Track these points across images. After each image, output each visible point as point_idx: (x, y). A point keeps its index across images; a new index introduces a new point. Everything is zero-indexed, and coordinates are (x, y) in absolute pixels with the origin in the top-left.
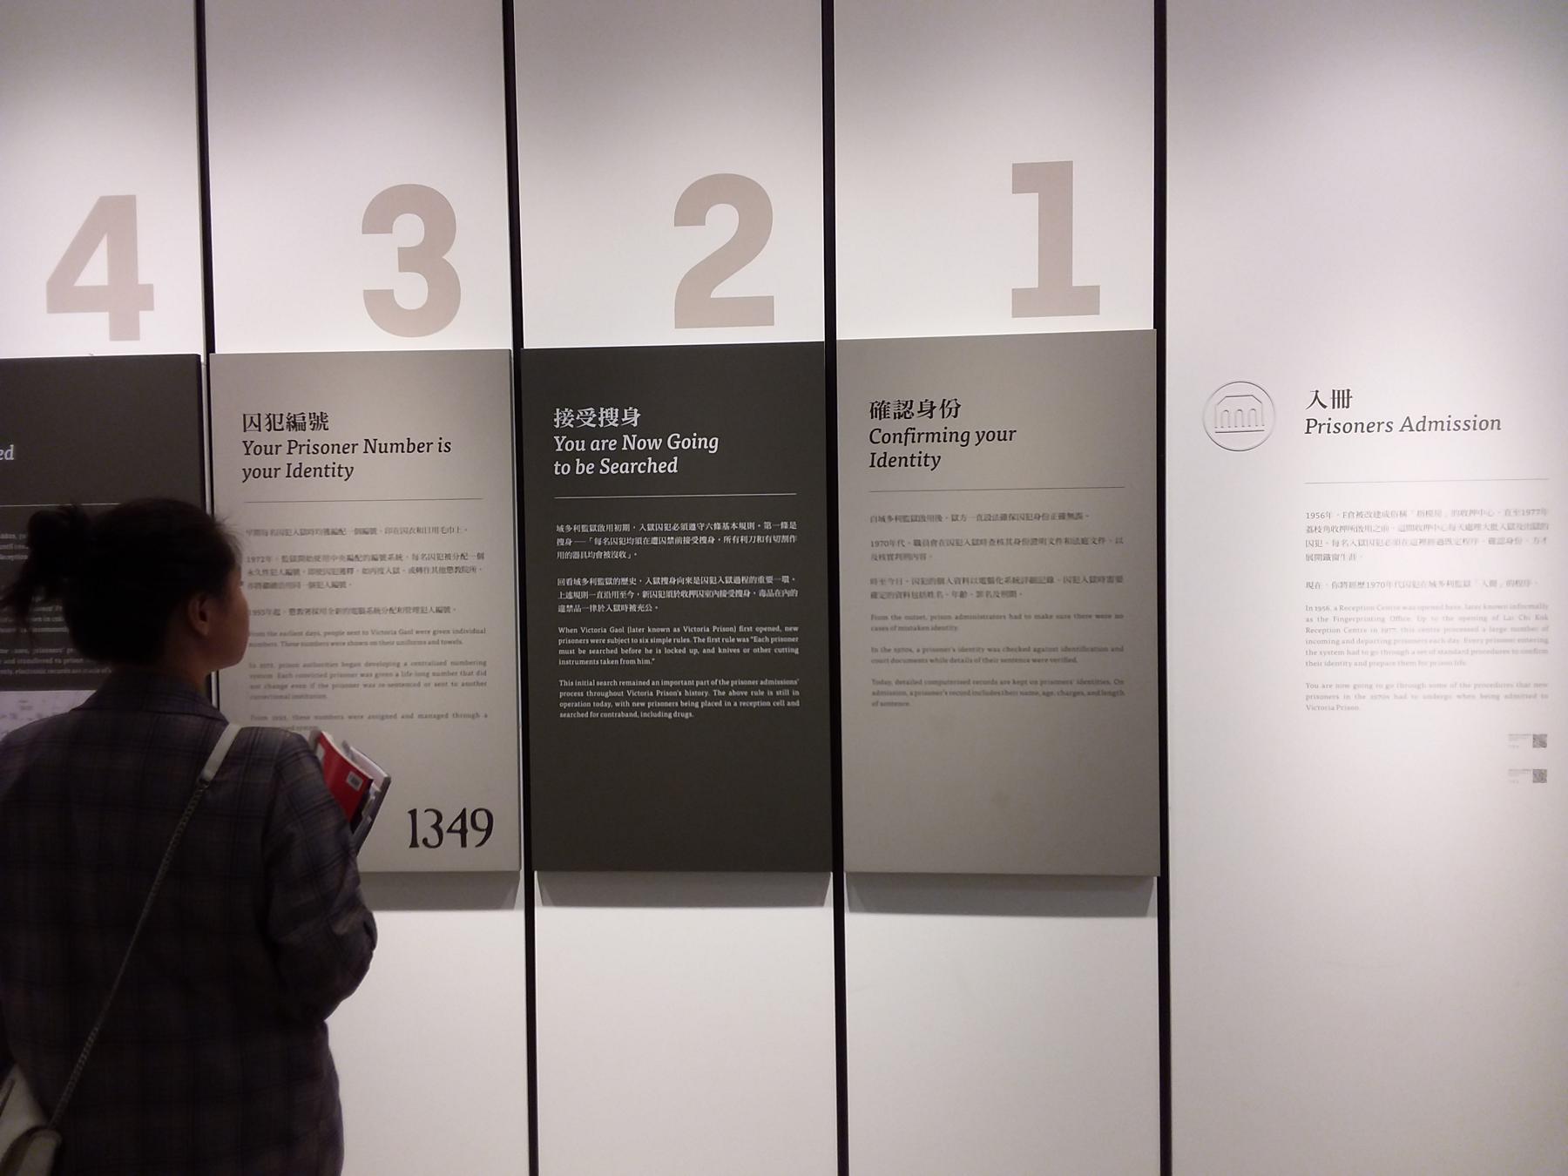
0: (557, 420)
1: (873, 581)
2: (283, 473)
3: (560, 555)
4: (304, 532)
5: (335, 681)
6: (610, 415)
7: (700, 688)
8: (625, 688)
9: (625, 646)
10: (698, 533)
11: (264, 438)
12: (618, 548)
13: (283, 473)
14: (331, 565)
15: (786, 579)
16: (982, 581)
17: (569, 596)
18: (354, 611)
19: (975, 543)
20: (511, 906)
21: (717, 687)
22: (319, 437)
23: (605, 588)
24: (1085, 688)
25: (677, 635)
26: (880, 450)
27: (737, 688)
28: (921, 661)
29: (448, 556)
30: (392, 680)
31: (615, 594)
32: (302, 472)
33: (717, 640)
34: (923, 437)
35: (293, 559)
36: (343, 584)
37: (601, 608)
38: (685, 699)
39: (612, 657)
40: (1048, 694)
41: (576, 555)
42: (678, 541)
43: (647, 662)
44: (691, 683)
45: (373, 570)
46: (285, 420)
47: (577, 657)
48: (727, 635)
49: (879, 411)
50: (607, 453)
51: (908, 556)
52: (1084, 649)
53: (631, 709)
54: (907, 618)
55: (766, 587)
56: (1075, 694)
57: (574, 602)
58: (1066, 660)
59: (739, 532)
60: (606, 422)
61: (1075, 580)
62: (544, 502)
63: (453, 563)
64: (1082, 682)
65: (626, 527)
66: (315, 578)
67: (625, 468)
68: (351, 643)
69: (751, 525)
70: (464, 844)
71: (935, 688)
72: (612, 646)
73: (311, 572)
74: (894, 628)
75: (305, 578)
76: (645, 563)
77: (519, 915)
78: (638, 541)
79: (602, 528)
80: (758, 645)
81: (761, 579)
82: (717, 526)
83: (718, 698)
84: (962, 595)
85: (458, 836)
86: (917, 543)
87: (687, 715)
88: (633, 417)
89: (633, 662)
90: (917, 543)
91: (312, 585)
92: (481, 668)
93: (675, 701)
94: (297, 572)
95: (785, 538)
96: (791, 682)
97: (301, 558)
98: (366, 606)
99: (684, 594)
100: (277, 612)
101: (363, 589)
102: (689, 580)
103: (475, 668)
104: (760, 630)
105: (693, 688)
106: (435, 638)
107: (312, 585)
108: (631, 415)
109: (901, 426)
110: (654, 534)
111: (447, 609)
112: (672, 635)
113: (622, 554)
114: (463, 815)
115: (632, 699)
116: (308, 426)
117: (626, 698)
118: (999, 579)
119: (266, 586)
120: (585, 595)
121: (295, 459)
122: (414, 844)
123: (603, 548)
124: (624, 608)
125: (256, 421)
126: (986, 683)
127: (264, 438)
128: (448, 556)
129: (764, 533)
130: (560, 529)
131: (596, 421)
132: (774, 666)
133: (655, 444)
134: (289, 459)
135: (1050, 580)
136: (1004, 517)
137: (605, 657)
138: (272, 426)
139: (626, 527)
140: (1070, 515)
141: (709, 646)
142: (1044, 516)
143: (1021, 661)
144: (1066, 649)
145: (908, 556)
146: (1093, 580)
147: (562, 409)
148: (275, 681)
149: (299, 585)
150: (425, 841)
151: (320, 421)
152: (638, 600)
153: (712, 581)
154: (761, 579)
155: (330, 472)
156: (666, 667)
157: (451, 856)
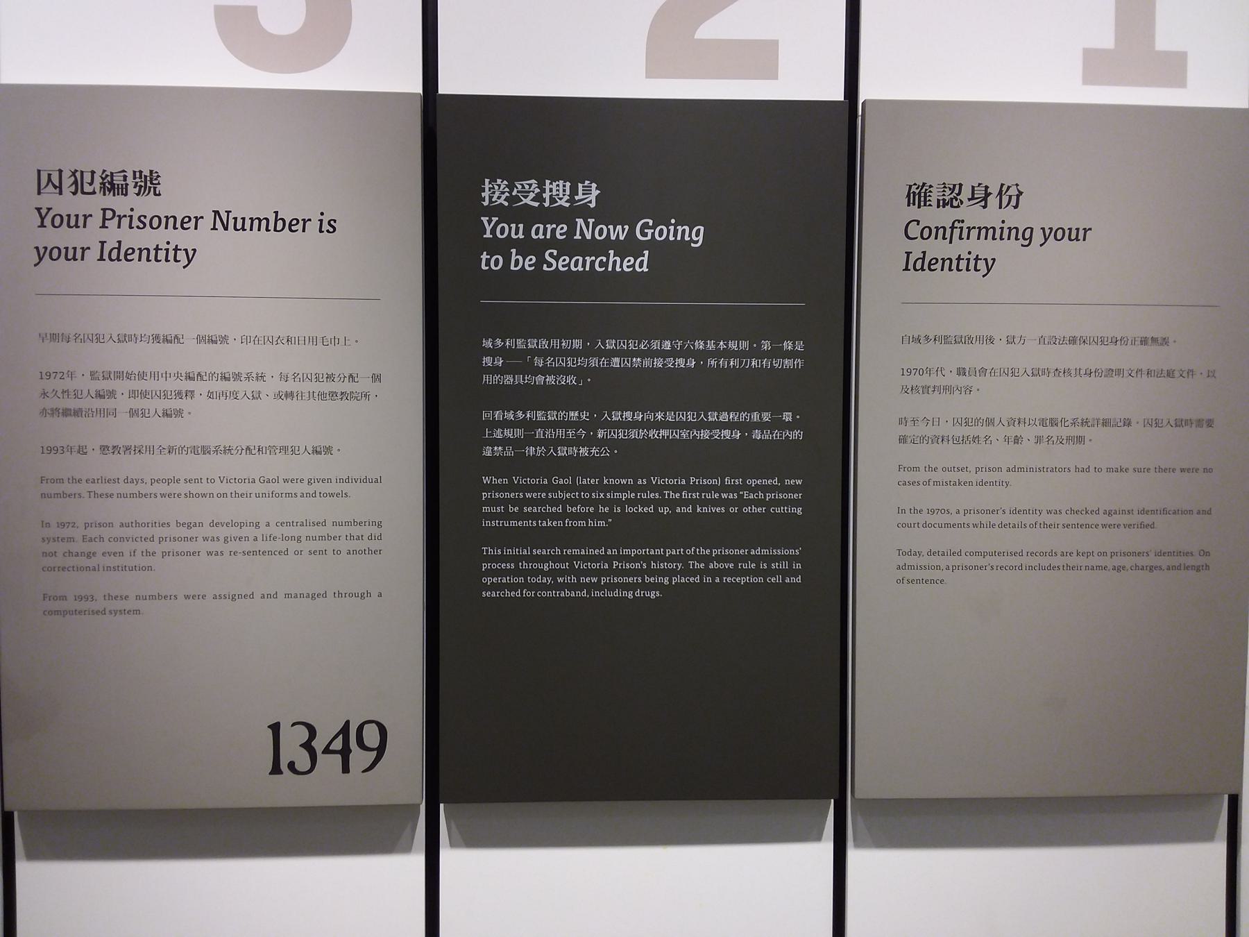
0: (486, 194)
1: (902, 421)
3: (487, 379)
4: (123, 339)
5: (166, 546)
6: (558, 191)
7: (672, 559)
8: (571, 558)
9: (573, 503)
10: (674, 353)
11: (68, 204)
12: (566, 371)
13: (94, 253)
14: (161, 385)
15: (787, 417)
16: (1043, 422)
17: (498, 434)
18: (194, 450)
19: (1036, 373)
20: (407, 849)
21: (696, 557)
22: (147, 205)
23: (546, 425)
24: (1164, 561)
25: (643, 489)
26: (917, 248)
27: (720, 559)
28: (961, 525)
29: (330, 377)
30: (247, 546)
31: (560, 432)
32: (121, 254)
33: (695, 496)
34: (974, 233)
35: (107, 376)
36: (179, 413)
37: (540, 450)
38: (652, 573)
39: (554, 516)
40: (1118, 569)
41: (509, 380)
42: (647, 363)
43: (602, 523)
44: (660, 552)
45: (223, 394)
46: (98, 180)
47: (507, 516)
48: (708, 489)
49: (918, 196)
50: (552, 242)
51: (948, 389)
52: (1165, 511)
53: (578, 586)
54: (944, 469)
55: (761, 426)
56: (1151, 569)
57: (504, 442)
58: (1142, 526)
59: (728, 354)
60: (553, 200)
61: (1157, 423)
62: (465, 309)
63: (337, 387)
64: (1160, 554)
65: (577, 344)
66: (138, 403)
67: (578, 264)
68: (189, 495)
69: (744, 345)
70: (346, 769)
71: (978, 561)
72: (555, 503)
73: (133, 394)
74: (927, 483)
75: (123, 403)
76: (601, 392)
77: (416, 862)
78: (594, 362)
79: (544, 344)
80: (750, 503)
81: (755, 416)
82: (699, 345)
83: (694, 573)
84: (1017, 440)
85: (338, 758)
86: (961, 372)
87: (653, 595)
88: (590, 195)
89: (582, 523)
90: (961, 372)
91: (133, 413)
92: (375, 530)
93: (638, 577)
94: (112, 394)
95: (788, 363)
96: (791, 552)
97: (119, 375)
98: (212, 444)
99: (653, 433)
100: (82, 450)
101: (209, 420)
102: (660, 416)
103: (366, 531)
104: (752, 482)
105: (662, 559)
106: (311, 490)
107: (133, 413)
108: (587, 191)
109: (945, 217)
110: (614, 353)
111: (328, 450)
112: (635, 488)
113: (571, 380)
114: (345, 730)
115: (580, 573)
116: (132, 190)
117: (572, 571)
118: (1063, 420)
119: (66, 413)
120: (519, 433)
121: (112, 235)
122: (276, 770)
123: (545, 371)
124: (573, 451)
125: (56, 181)
126: (1043, 554)
127: (68, 204)
128: (330, 377)
129: (761, 355)
130: (488, 344)
131: (539, 198)
132: (770, 530)
133: (619, 232)
134: (104, 235)
135: (1127, 423)
136: (1073, 341)
137: (544, 516)
138: (78, 188)
139: (577, 344)
140: (1154, 340)
141: (685, 503)
142: (1123, 341)
143: (1088, 526)
144: (1143, 512)
145: (948, 389)
146: (1179, 423)
147: (493, 180)
148: (79, 546)
149: (115, 413)
150: (291, 766)
151: (149, 183)
152: (591, 441)
153: (690, 417)
154: (755, 416)
156: (627, 530)
157: (327, 785)
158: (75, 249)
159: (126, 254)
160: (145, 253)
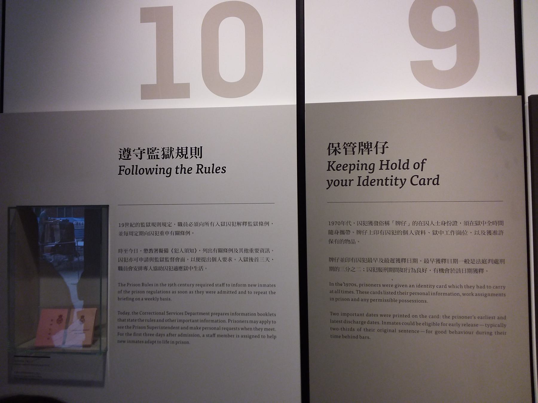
2: (355, 183)
13: (355, 183)
127: (341, 159)
155: (389, 182)
158: (346, 180)
159: (371, 182)
160: (380, 181)
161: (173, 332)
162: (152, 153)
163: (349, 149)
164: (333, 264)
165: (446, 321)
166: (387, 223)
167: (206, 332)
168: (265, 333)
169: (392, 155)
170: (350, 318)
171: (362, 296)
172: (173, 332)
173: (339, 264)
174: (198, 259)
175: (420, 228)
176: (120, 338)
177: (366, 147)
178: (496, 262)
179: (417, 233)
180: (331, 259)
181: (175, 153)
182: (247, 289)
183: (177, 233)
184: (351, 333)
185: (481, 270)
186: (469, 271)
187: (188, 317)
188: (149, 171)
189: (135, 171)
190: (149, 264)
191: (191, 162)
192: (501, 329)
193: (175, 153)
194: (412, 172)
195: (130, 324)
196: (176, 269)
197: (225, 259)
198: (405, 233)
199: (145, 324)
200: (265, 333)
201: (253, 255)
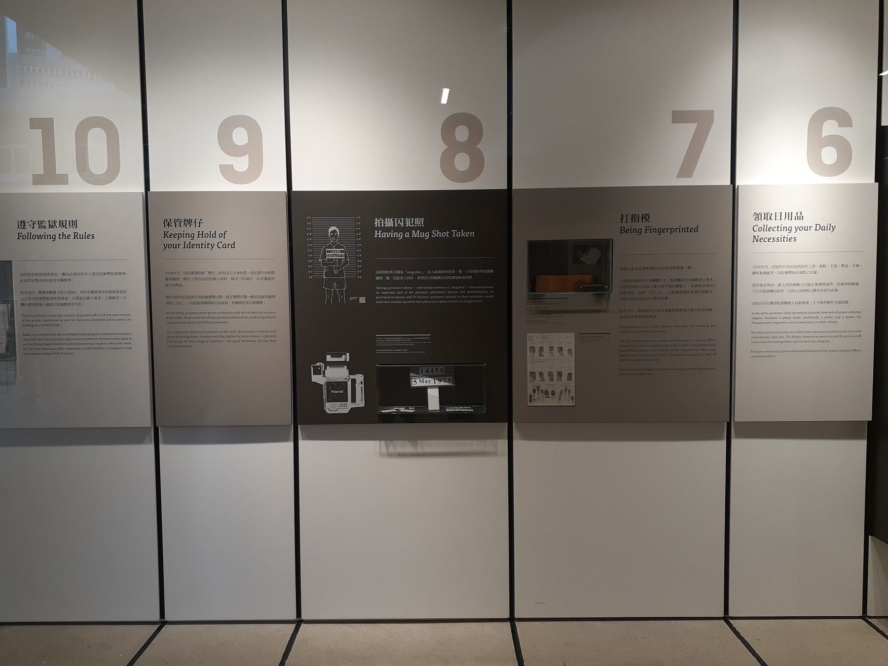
13: (182, 246)
127: (172, 230)
161: (62, 346)
162: (41, 224)
163: (178, 223)
164: (168, 300)
165: (240, 334)
166: (203, 273)
167: (85, 346)
168: (124, 346)
169: (205, 228)
170: (179, 335)
171: (187, 320)
172: (62, 346)
173: (173, 300)
174: (77, 298)
175: (223, 276)
176: (25, 352)
177: (189, 222)
178: (270, 297)
179: (222, 279)
180: (167, 297)
181: (57, 224)
182: (112, 317)
183: (62, 280)
184: (180, 344)
185: (261, 302)
186: (254, 303)
187: (72, 337)
188: (40, 237)
189: (30, 236)
190: (42, 302)
191: (69, 231)
192: (273, 339)
193: (57, 224)
194: (218, 239)
195: (32, 342)
196: (62, 305)
197: (96, 298)
198: (214, 279)
199: (43, 342)
200: (124, 346)
201: (115, 295)
